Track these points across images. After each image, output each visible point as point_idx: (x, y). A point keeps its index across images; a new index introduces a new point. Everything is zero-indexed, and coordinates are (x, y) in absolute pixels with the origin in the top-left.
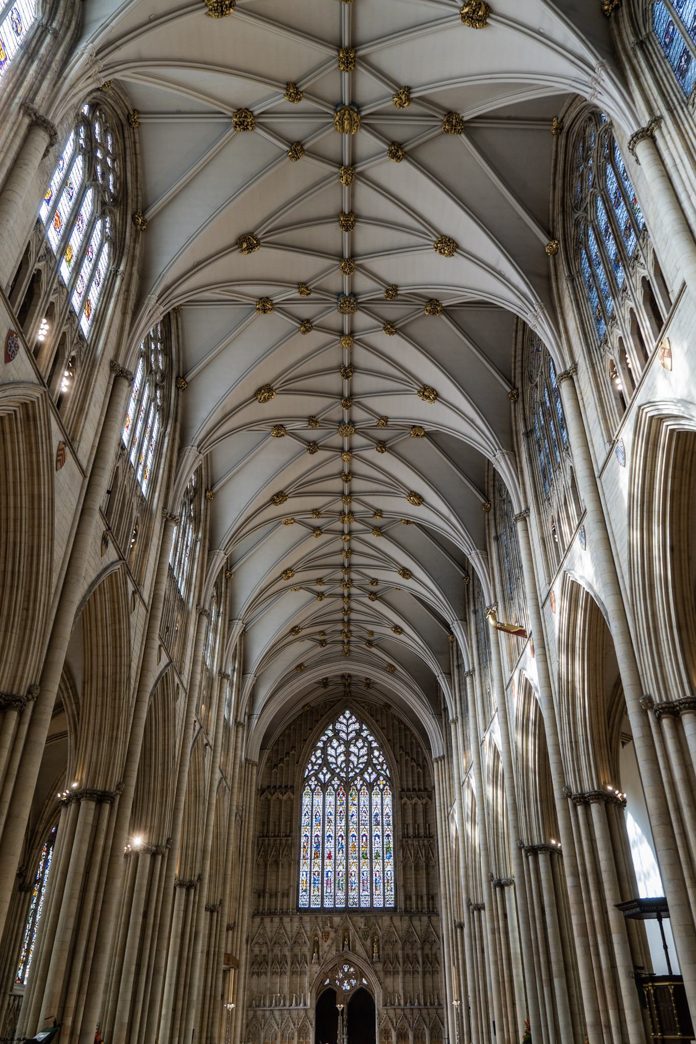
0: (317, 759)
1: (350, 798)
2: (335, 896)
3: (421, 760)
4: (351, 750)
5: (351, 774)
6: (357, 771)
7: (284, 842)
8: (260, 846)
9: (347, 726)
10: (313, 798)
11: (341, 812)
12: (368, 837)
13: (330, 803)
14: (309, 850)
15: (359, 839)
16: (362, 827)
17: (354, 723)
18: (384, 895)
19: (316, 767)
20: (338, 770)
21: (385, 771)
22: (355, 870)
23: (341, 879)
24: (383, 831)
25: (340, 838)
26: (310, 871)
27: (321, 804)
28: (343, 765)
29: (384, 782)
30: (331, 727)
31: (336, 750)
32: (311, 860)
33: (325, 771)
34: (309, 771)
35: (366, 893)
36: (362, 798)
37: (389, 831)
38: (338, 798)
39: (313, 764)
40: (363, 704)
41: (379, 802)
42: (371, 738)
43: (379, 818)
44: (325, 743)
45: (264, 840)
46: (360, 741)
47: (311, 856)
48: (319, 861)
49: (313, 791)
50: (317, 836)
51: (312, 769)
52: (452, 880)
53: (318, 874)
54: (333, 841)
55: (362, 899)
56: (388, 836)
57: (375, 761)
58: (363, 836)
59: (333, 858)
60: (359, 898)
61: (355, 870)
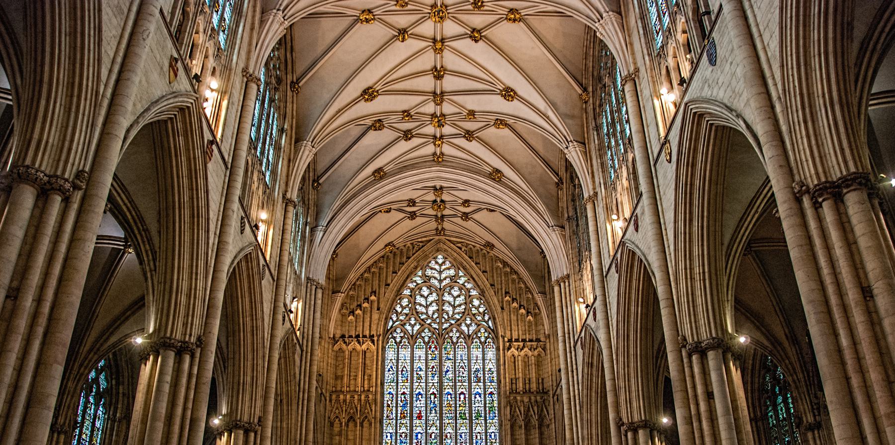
0: (403, 308)
3: (532, 306)
4: (444, 298)
5: (445, 326)
6: (453, 322)
7: (363, 397)
8: (333, 402)
9: (440, 272)
10: (398, 351)
11: (433, 367)
12: (467, 396)
13: (420, 357)
14: (394, 409)
15: (456, 398)
17: (449, 269)
20: (429, 321)
21: (487, 322)
22: (451, 431)
23: (435, 441)
24: (485, 388)
25: (432, 397)
26: (396, 433)
28: (436, 316)
29: (486, 335)
30: (420, 273)
31: (426, 298)
32: (397, 420)
34: (394, 322)
36: (460, 352)
37: (492, 388)
38: (430, 352)
40: (459, 245)
41: (480, 356)
43: (480, 375)
44: (412, 290)
45: (338, 396)
46: (456, 288)
47: (397, 416)
48: (407, 421)
50: (404, 393)
52: (582, 420)
53: (406, 436)
56: (491, 393)
57: (474, 311)
58: (460, 394)
59: (424, 418)
61: (451, 431)
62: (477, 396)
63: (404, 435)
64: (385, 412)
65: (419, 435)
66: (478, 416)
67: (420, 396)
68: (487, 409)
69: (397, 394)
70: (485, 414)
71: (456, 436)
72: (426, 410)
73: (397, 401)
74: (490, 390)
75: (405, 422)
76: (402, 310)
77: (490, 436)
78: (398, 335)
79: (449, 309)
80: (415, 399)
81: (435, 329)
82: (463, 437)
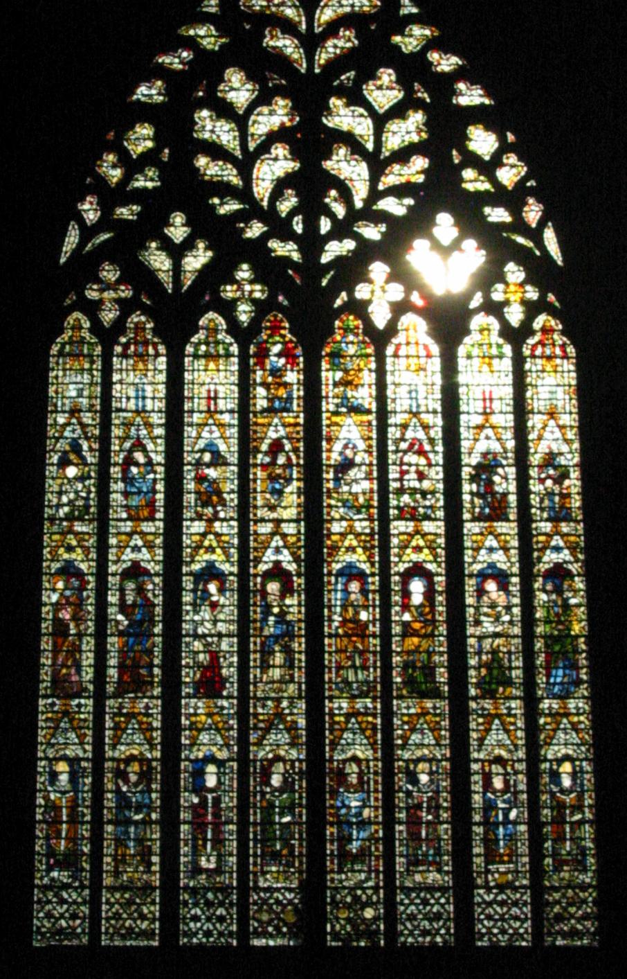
0: (132, 166)
1: (328, 376)
2: (244, 889)
4: (330, 122)
5: (335, 250)
6: (372, 233)
10: (107, 371)
11: (276, 447)
14: (88, 644)
15: (385, 590)
16: (399, 527)
18: (537, 889)
19: (125, 212)
20: (255, 230)
25: (273, 587)
27: (156, 404)
31: (241, 121)
32: (100, 697)
33: (178, 230)
34: (87, 232)
35: (433, 877)
39: (111, 197)
42: (446, 63)
46: (387, 76)
48: (151, 704)
49: (107, 336)
50: (135, 572)
51: (106, 221)
53: (145, 776)
54: (228, 602)
55: (407, 906)
56: (558, 574)
57: (472, 181)
58: (407, 576)
59: (232, 688)
60: (390, 904)
62: (491, 586)
63: (135, 767)
64: (46, 660)
65: (211, 768)
66: (495, 678)
67: (212, 588)
68: (539, 645)
69: (102, 573)
70: (529, 669)
71: (388, 773)
72: (243, 652)
73: (102, 604)
74: (550, 558)
75: (141, 705)
76: (127, 178)
77: (555, 776)
78: (106, 295)
79: (353, 172)
80: (187, 598)
81: (286, 261)
82: (424, 778)
